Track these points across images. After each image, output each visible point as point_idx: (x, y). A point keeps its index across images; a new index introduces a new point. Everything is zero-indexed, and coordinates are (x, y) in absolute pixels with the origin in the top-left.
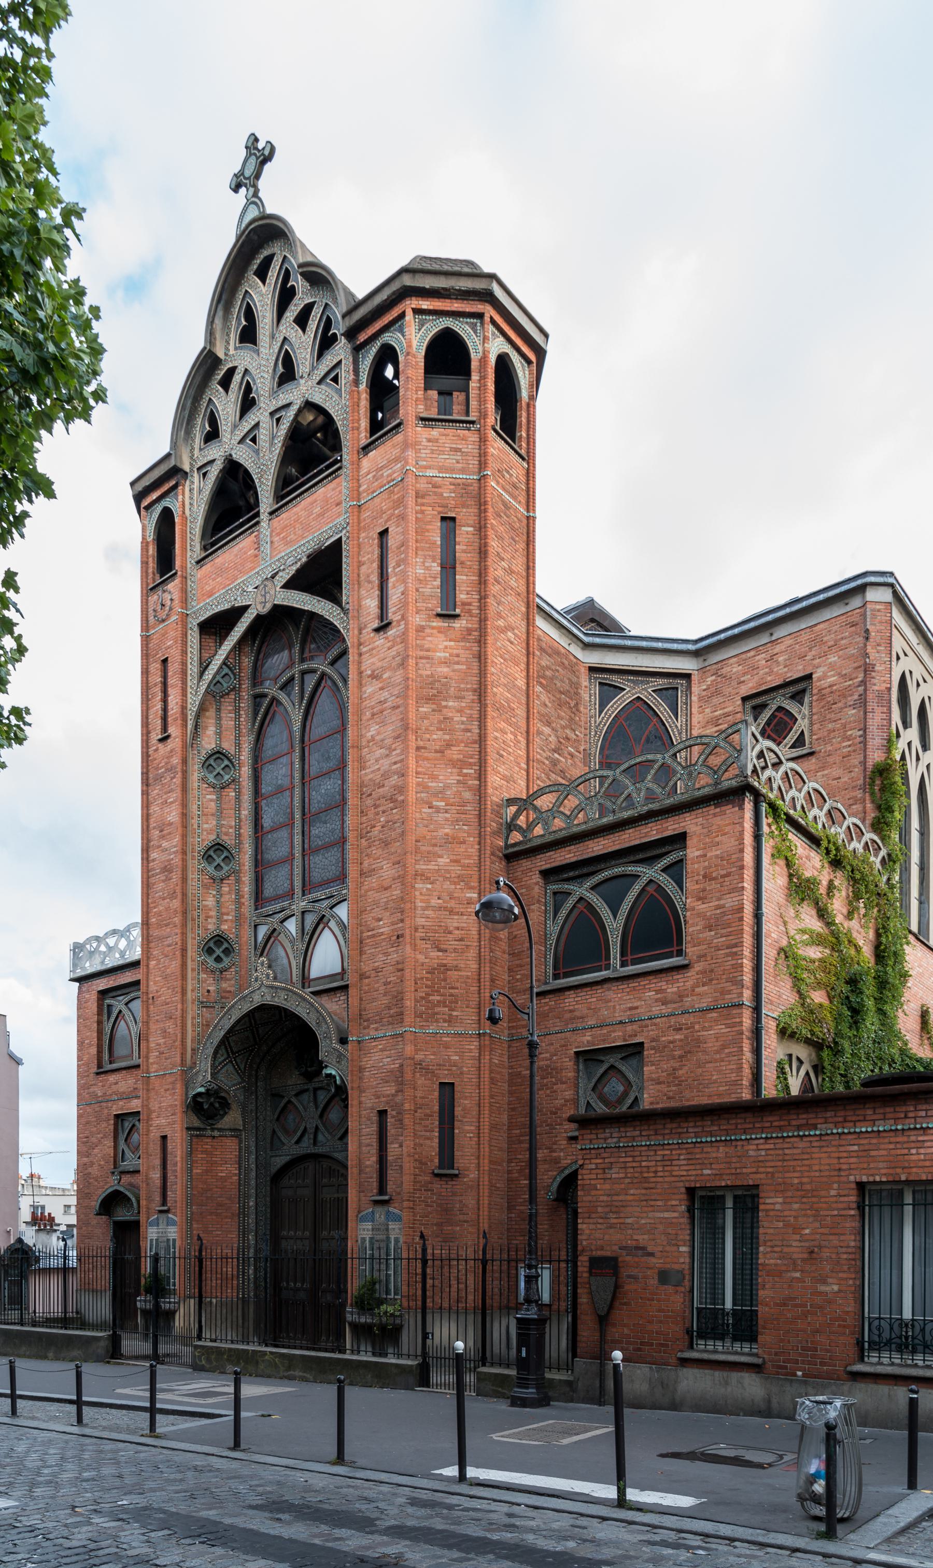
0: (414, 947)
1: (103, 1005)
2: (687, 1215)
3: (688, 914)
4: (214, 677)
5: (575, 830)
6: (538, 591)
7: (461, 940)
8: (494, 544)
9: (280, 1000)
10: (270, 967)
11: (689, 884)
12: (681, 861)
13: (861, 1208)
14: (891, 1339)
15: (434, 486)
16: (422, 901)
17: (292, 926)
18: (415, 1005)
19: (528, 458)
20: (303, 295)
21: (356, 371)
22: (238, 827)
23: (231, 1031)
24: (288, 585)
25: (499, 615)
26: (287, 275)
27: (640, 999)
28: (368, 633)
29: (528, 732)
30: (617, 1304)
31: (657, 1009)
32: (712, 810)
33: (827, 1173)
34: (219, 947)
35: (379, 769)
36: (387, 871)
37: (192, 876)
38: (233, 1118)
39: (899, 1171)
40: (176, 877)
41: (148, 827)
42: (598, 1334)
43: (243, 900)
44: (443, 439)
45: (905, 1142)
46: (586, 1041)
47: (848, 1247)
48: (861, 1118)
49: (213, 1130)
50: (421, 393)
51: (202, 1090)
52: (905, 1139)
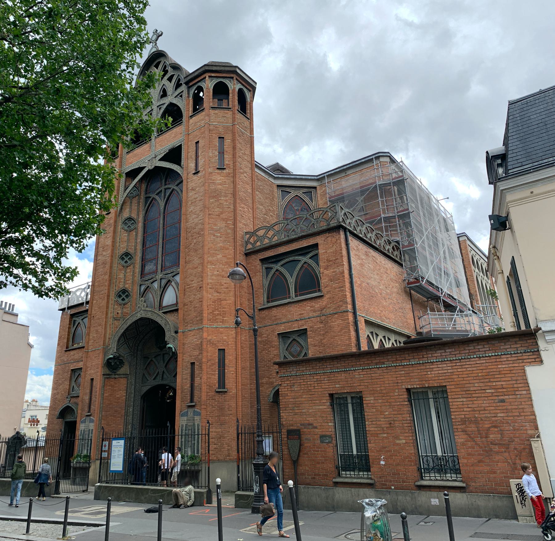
0: (207, 292)
1: (72, 320)
2: (330, 407)
3: (321, 275)
4: (130, 191)
5: (273, 243)
6: (255, 160)
7: (227, 288)
8: (238, 145)
9: (149, 315)
10: (145, 302)
11: (321, 264)
12: (317, 254)
13: (410, 401)
14: (434, 467)
15: (216, 127)
16: (210, 272)
17: (156, 285)
18: (208, 316)
19: (250, 119)
20: (171, 72)
21: (188, 94)
22: (136, 246)
23: (127, 329)
24: (160, 160)
25: (241, 168)
26: (165, 67)
27: (304, 310)
28: (191, 175)
29: (253, 208)
30: (301, 454)
31: (311, 315)
32: (327, 235)
33: (392, 385)
34: (124, 294)
35: (194, 222)
36: (196, 261)
37: (115, 266)
38: (125, 369)
39: (424, 382)
40: (108, 266)
41: (98, 247)
42: (293, 471)
43: (136, 275)
44: (219, 113)
45: (424, 369)
46: (282, 329)
47: (407, 420)
48: (404, 359)
49: (115, 375)
50: (211, 100)
51: (112, 356)
52: (424, 367)
